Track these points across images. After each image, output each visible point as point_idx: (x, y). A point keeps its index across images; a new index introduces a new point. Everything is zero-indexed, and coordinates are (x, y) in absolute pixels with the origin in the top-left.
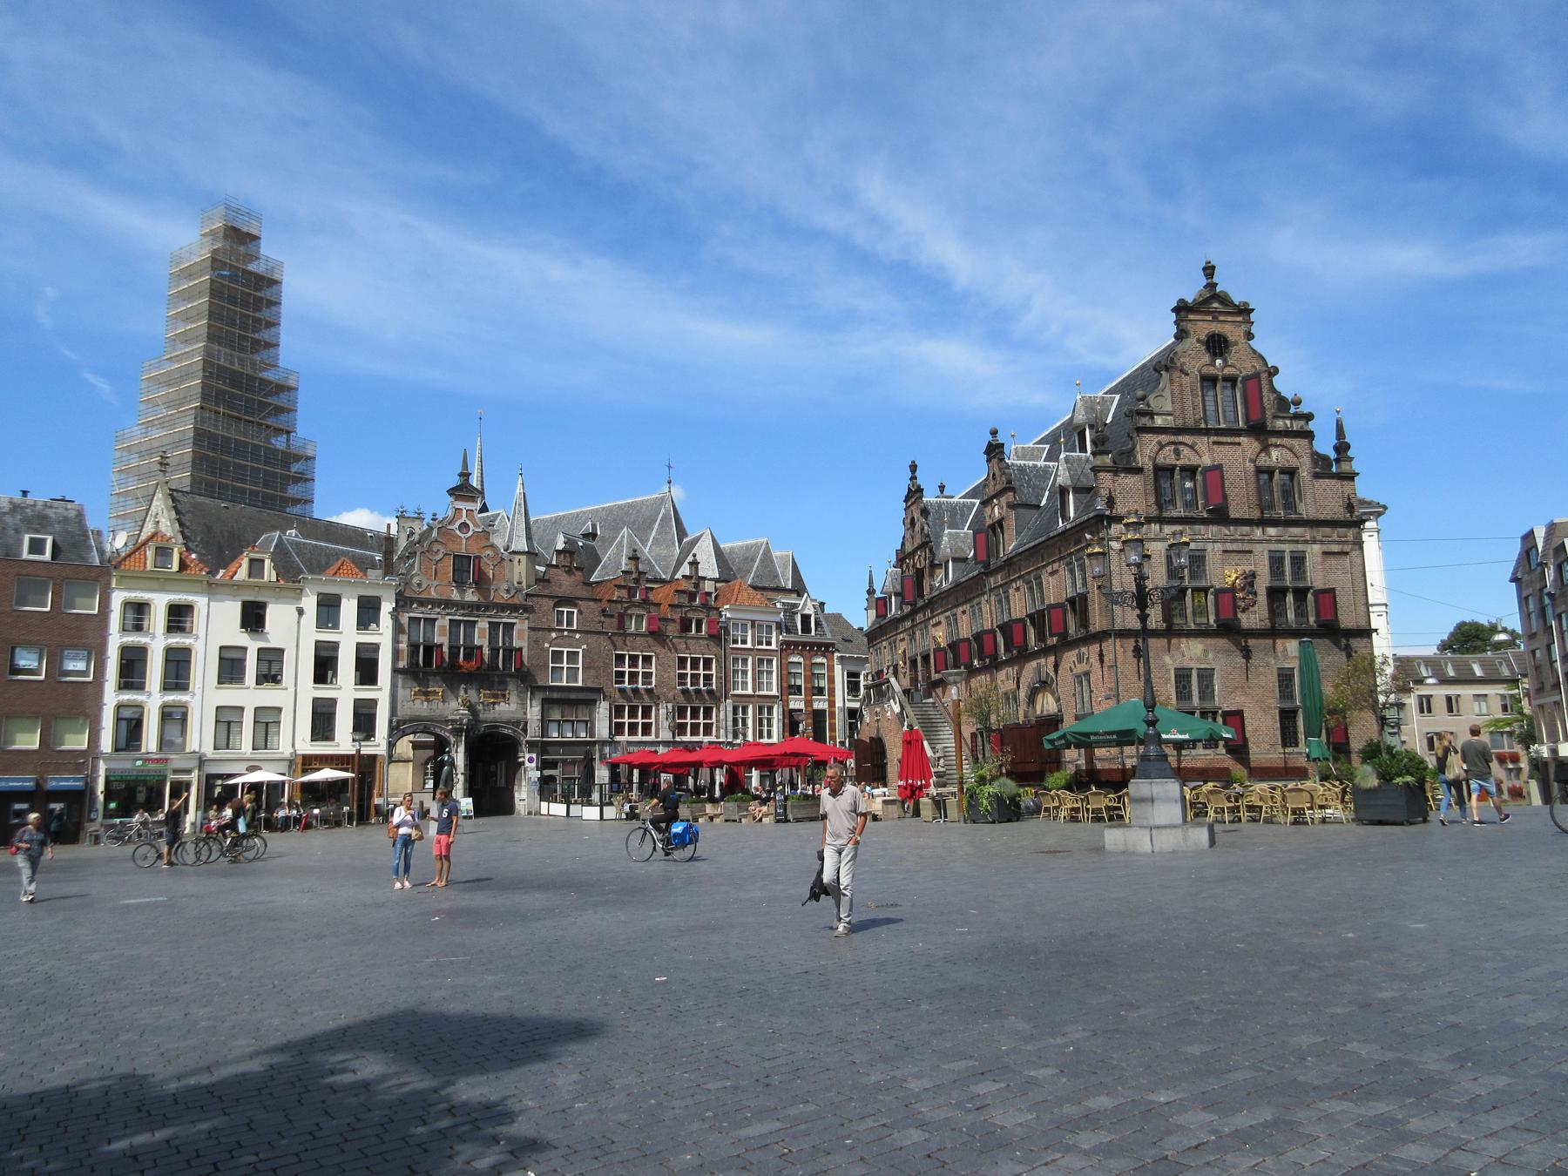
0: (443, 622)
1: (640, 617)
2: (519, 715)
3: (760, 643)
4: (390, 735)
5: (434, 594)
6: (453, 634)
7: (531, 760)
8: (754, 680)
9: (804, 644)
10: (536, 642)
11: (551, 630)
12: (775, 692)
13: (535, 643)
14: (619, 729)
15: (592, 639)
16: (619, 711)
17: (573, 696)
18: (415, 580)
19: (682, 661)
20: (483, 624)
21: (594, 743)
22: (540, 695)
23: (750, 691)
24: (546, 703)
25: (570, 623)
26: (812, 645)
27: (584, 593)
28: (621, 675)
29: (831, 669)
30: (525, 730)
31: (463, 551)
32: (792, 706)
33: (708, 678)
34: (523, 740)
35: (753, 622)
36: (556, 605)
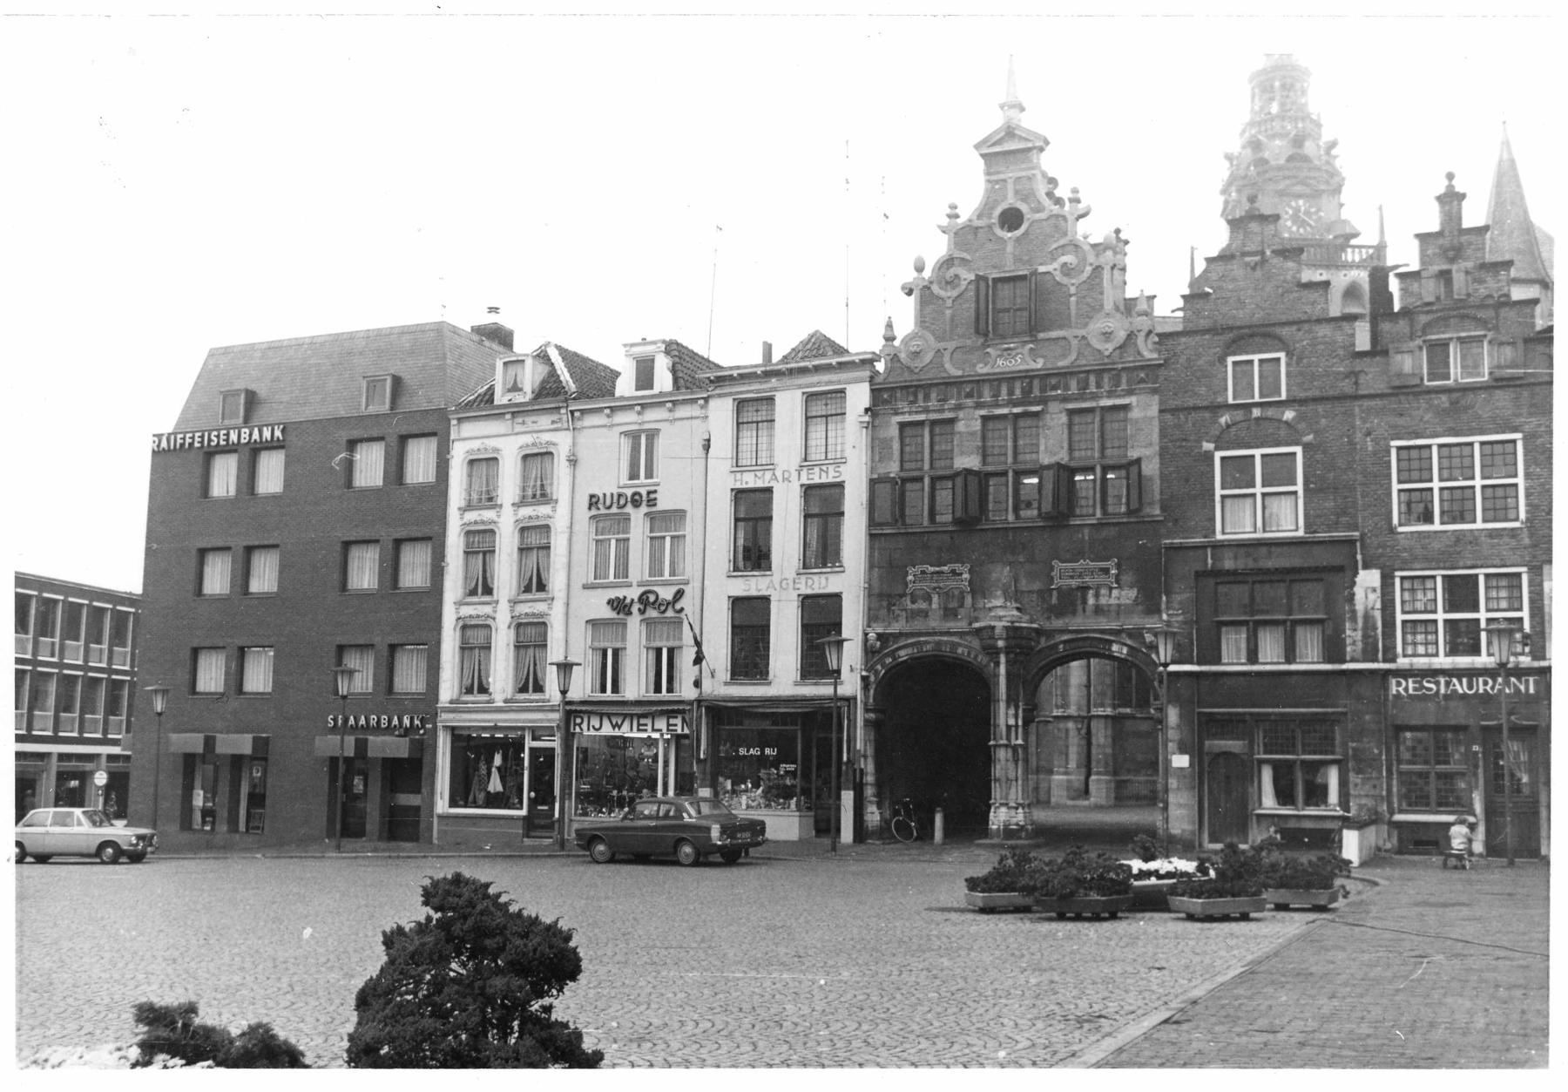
0: (969, 423)
20: (1056, 418)
25: (1270, 385)
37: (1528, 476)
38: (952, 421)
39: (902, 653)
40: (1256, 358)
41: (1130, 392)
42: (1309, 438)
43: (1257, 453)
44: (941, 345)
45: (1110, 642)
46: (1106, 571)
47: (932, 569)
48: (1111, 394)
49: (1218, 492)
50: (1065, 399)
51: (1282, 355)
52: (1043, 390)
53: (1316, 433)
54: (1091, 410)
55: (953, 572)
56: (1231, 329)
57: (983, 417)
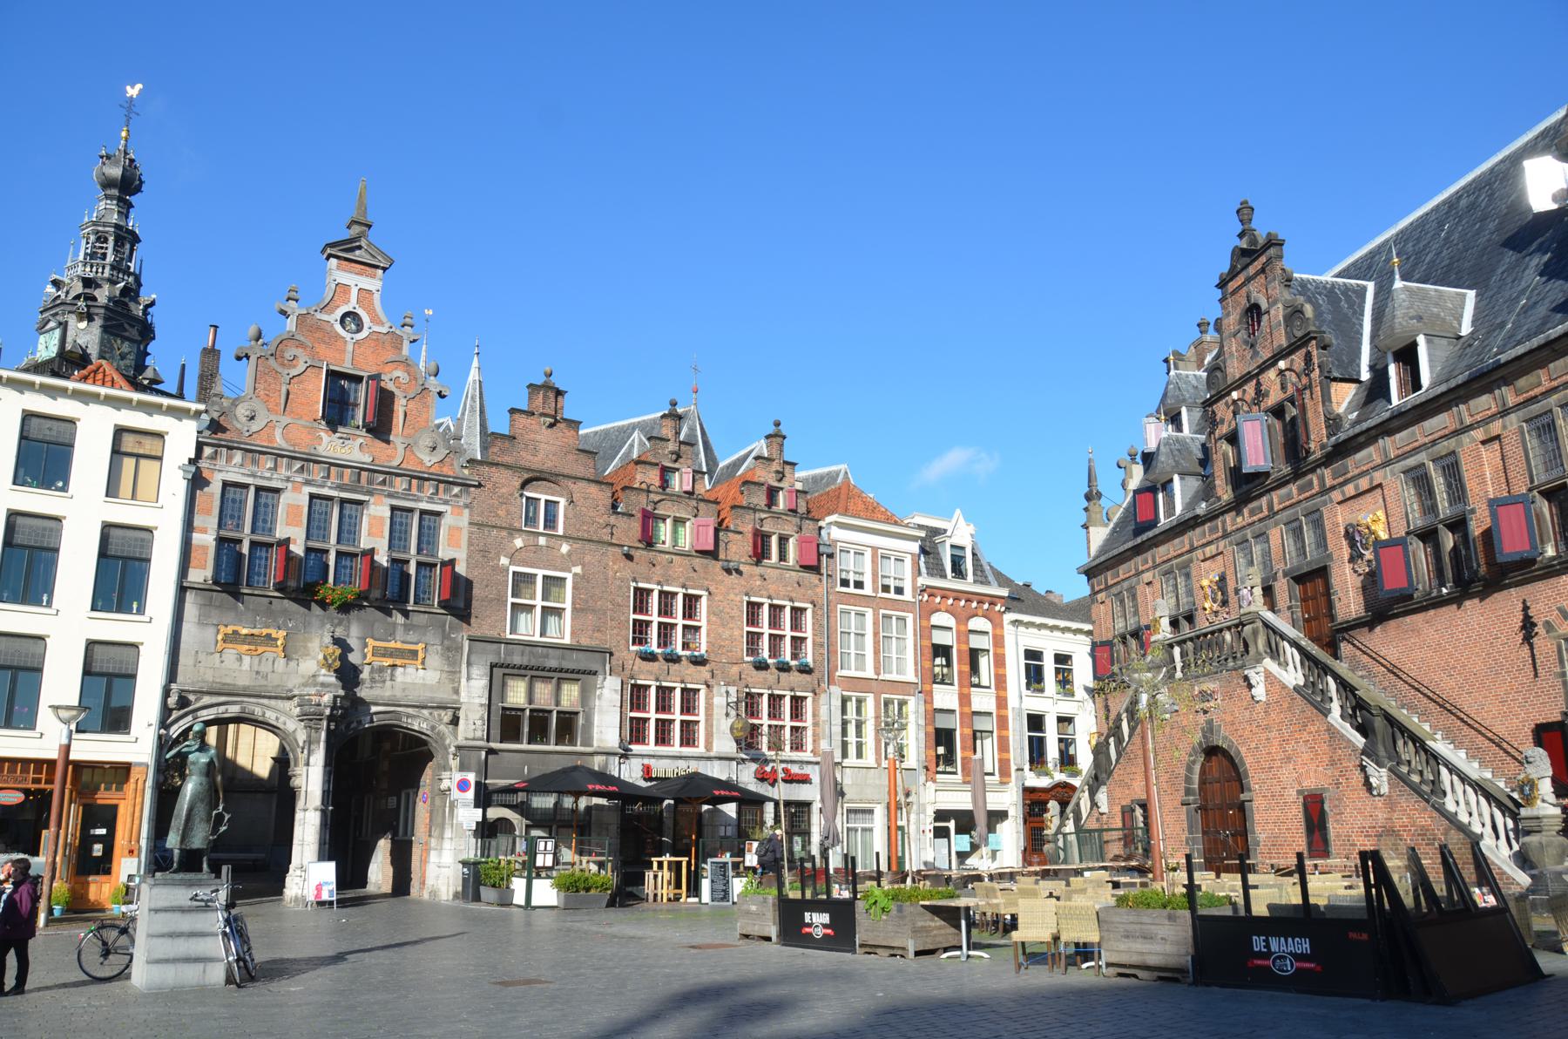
1: (679, 522)
2: (444, 695)
3: (886, 588)
4: (164, 723)
5: (279, 441)
6: (315, 525)
7: (463, 785)
8: (876, 652)
9: (958, 595)
10: (484, 552)
11: (513, 531)
12: (910, 676)
13: (482, 552)
14: (636, 731)
15: (592, 555)
16: (637, 695)
17: (553, 663)
18: (242, 411)
19: (754, 608)
21: (592, 754)
22: (490, 655)
23: (869, 673)
24: (500, 673)
25: (550, 521)
26: (969, 597)
27: (580, 471)
28: (641, 628)
29: (999, 641)
30: (455, 721)
31: (346, 367)
32: (937, 704)
33: (797, 642)
34: (451, 743)
35: (875, 549)
36: (524, 485)
37: (708, 621)
38: (277, 491)
39: (204, 712)
40: (543, 497)
41: (446, 502)
42: (578, 569)
43: (540, 573)
44: (274, 418)
45: (408, 716)
46: (414, 654)
47: (245, 631)
48: (431, 500)
49: (511, 600)
50: (390, 495)
51: (562, 502)
52: (370, 482)
53: (583, 566)
54: (411, 510)
55: (269, 635)
56: (529, 470)
57: (312, 497)
